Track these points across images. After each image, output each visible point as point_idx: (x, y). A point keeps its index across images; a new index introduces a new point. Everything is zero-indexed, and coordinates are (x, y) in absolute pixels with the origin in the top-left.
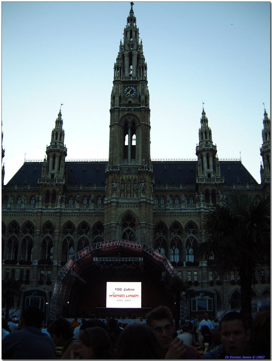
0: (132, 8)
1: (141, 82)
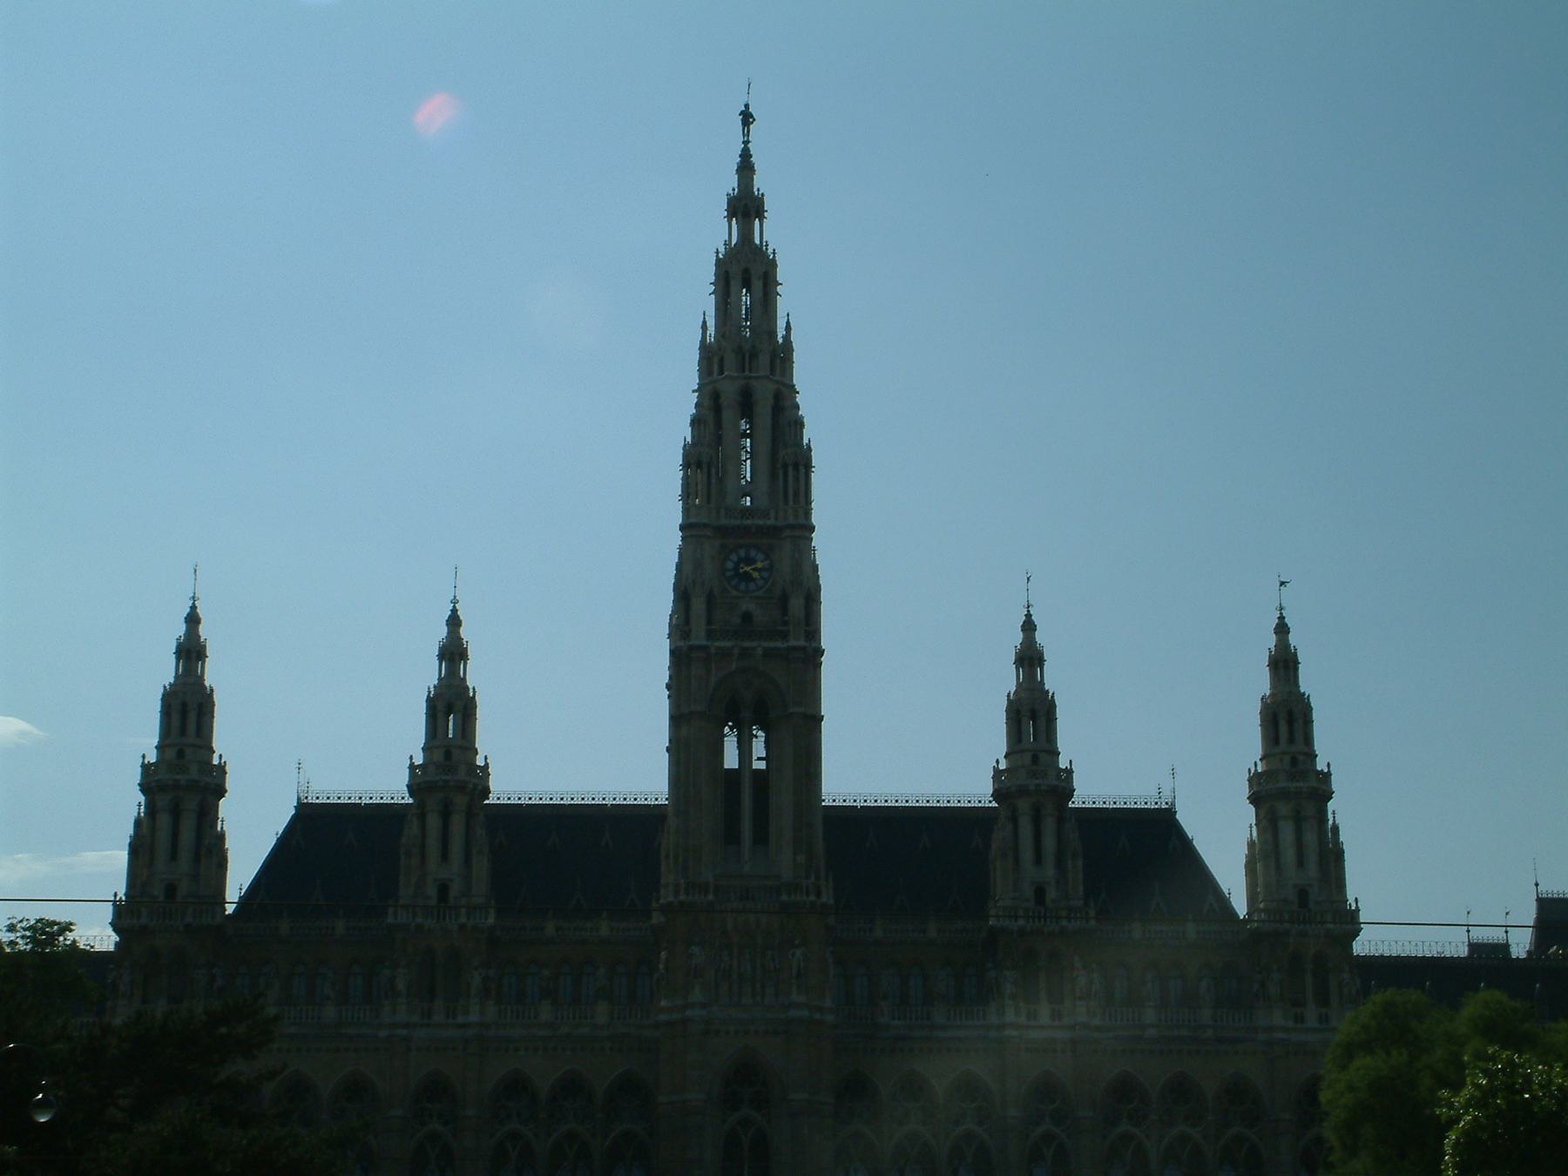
0: (746, 143)
1: (788, 533)
